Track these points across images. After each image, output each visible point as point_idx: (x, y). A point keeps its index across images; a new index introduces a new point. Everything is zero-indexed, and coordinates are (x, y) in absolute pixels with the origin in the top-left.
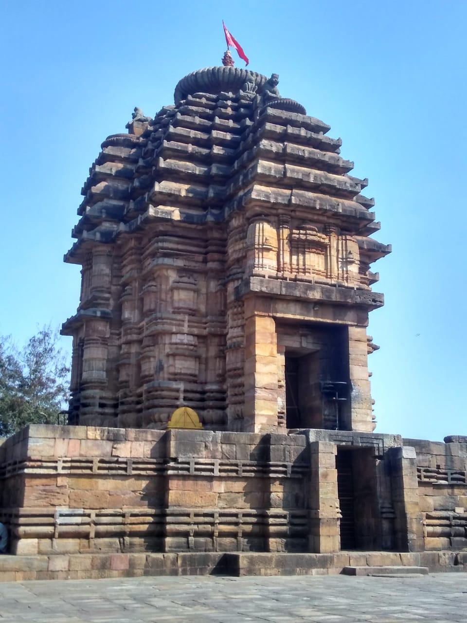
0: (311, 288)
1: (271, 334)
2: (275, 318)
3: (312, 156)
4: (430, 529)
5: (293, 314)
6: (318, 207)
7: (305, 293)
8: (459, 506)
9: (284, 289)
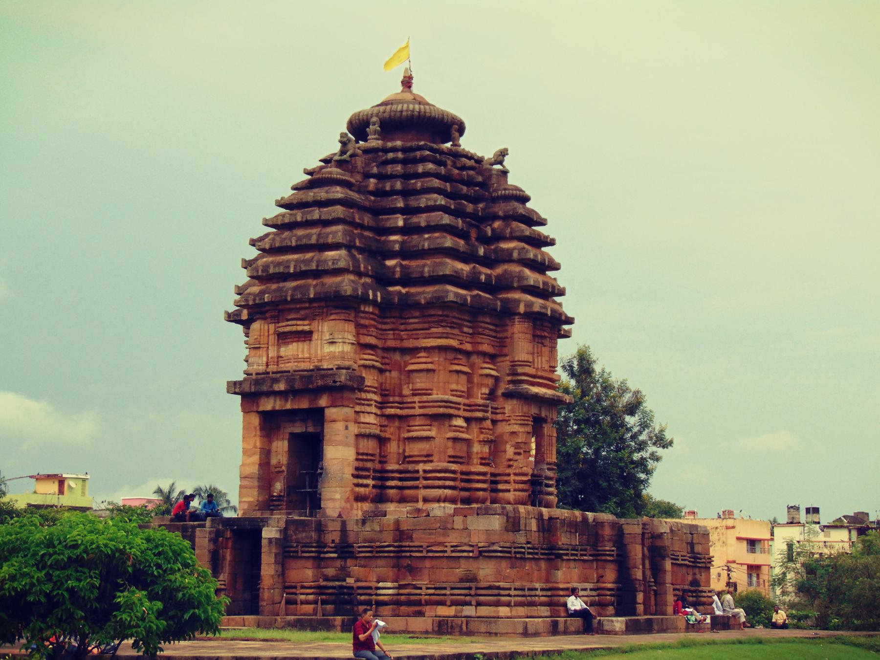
0: (276, 381)
1: (255, 428)
2: (258, 412)
3: (299, 243)
4: (303, 597)
5: (268, 405)
6: (289, 299)
7: (271, 386)
8: (349, 576)
9: (253, 387)
